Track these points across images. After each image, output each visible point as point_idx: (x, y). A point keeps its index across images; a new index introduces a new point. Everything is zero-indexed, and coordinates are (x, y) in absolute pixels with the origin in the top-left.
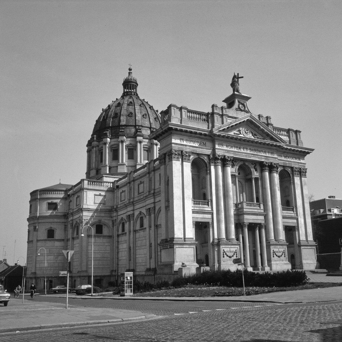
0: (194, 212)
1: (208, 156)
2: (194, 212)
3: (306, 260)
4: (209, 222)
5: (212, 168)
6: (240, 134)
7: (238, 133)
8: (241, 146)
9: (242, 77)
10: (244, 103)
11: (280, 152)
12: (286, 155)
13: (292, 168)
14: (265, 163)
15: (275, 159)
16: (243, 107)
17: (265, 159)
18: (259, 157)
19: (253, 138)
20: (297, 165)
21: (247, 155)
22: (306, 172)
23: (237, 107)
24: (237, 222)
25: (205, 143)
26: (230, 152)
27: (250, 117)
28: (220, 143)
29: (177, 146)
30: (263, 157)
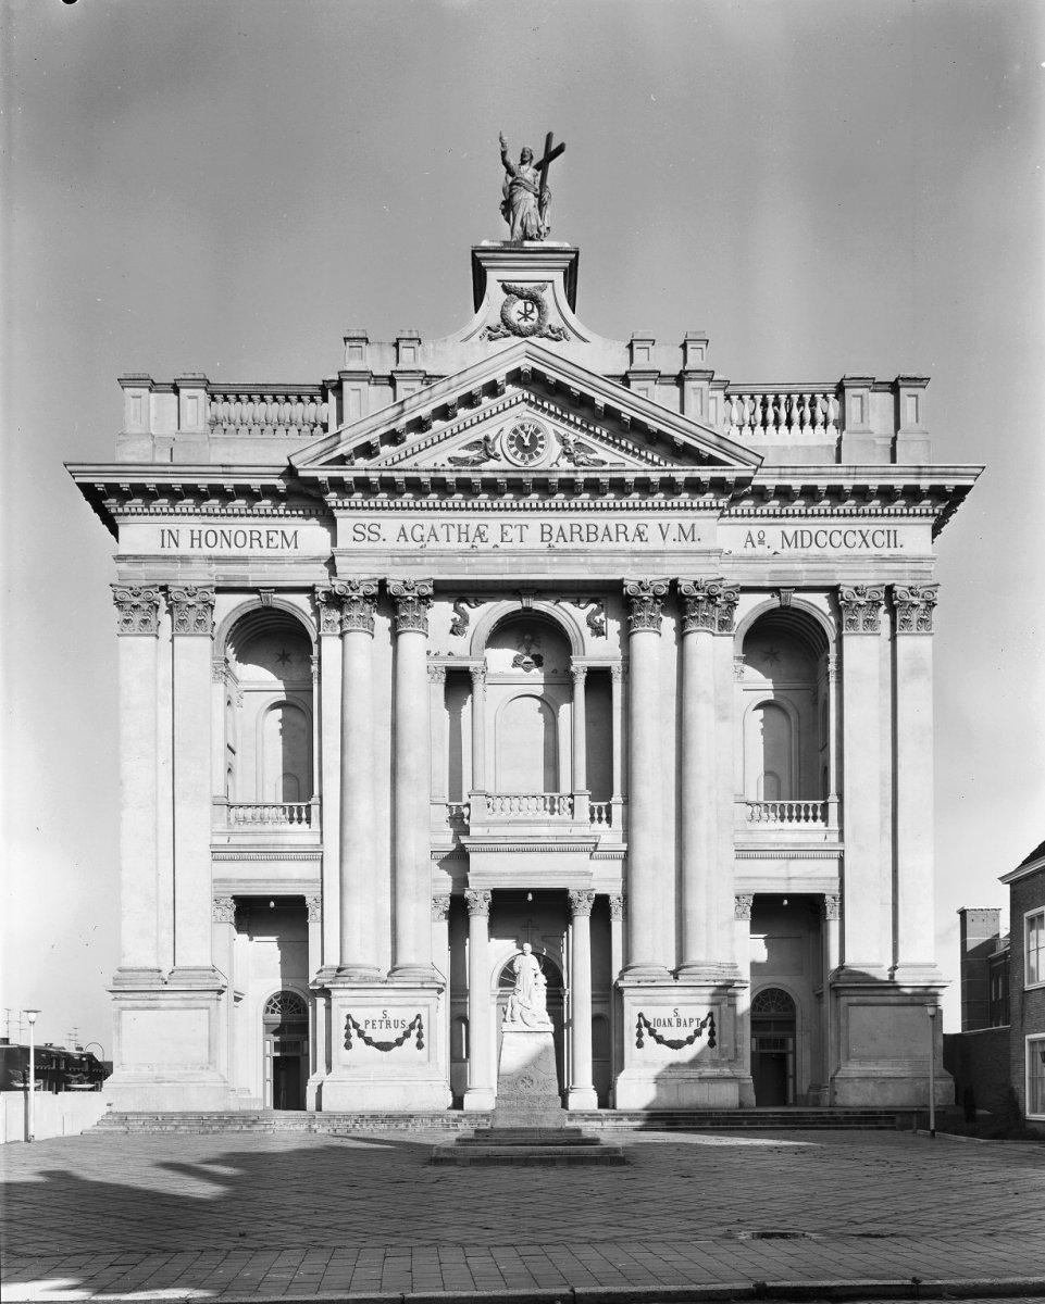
0: (218, 854)
1: (310, 590)
2: (218, 854)
3: (863, 1059)
4: (301, 900)
5: (330, 648)
6: (484, 461)
7: (473, 454)
8: (484, 522)
9: (561, 149)
10: (542, 290)
11: (753, 520)
12: (799, 528)
13: (833, 591)
14: (630, 588)
15: (702, 560)
16: (535, 315)
17: (634, 565)
18: (597, 560)
19: (571, 466)
20: (872, 575)
21: (524, 560)
22: (931, 605)
23: (495, 320)
24: (455, 893)
25: (295, 533)
26: (418, 560)
27: (529, 356)
28: (363, 521)
29: (144, 567)
30: (623, 560)
